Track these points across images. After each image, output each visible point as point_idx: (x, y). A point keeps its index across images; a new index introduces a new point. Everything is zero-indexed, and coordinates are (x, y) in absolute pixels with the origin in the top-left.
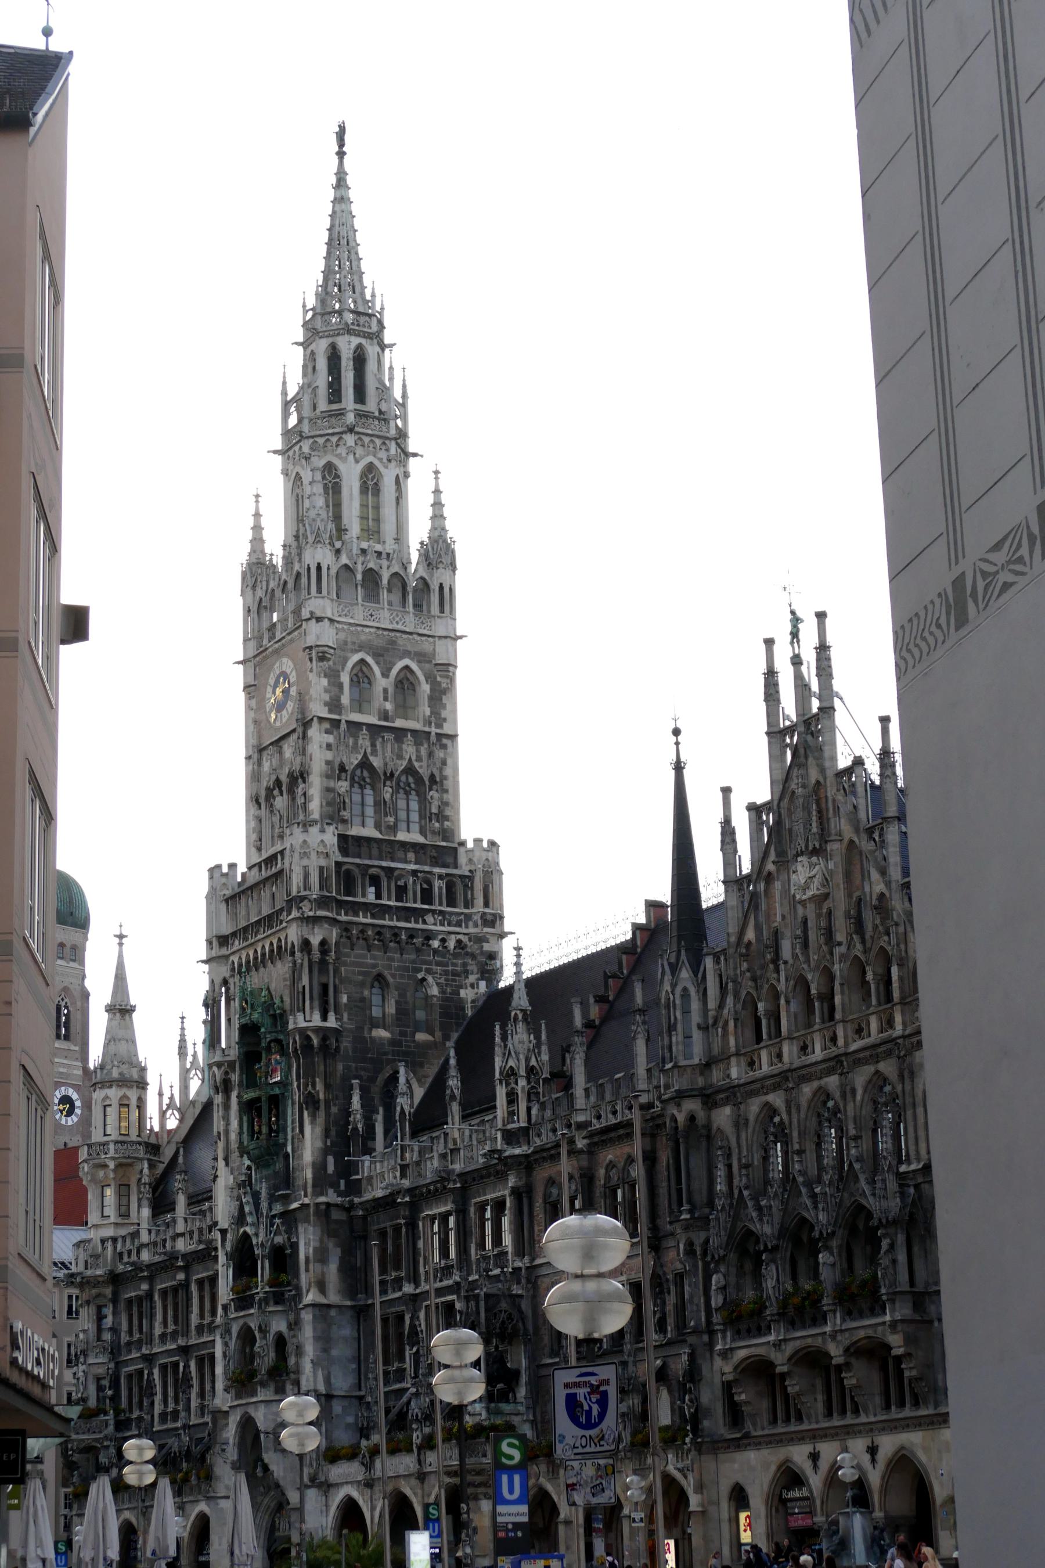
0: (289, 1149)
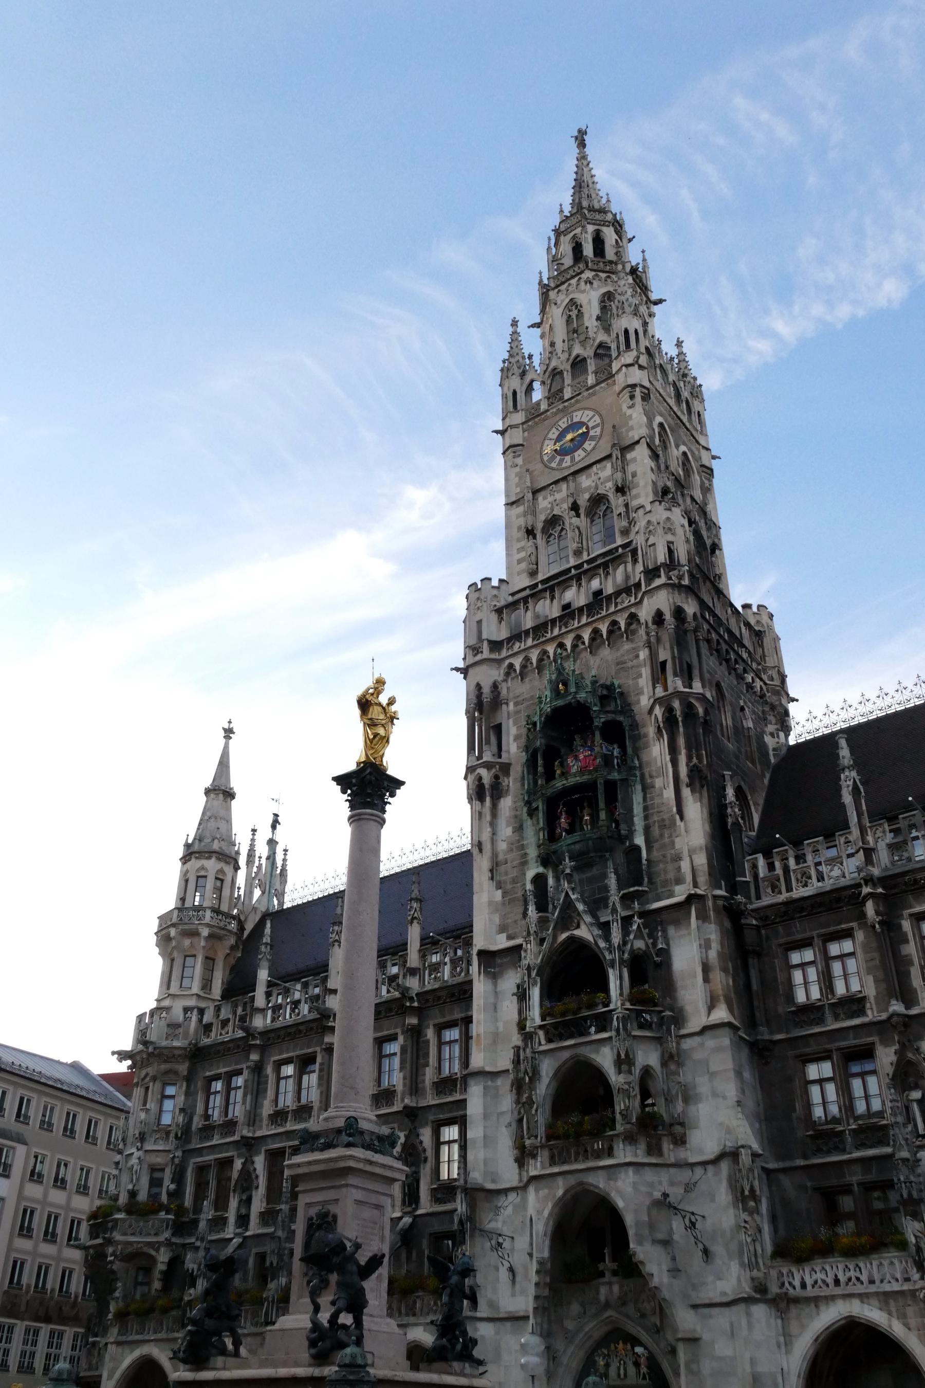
0: (639, 840)
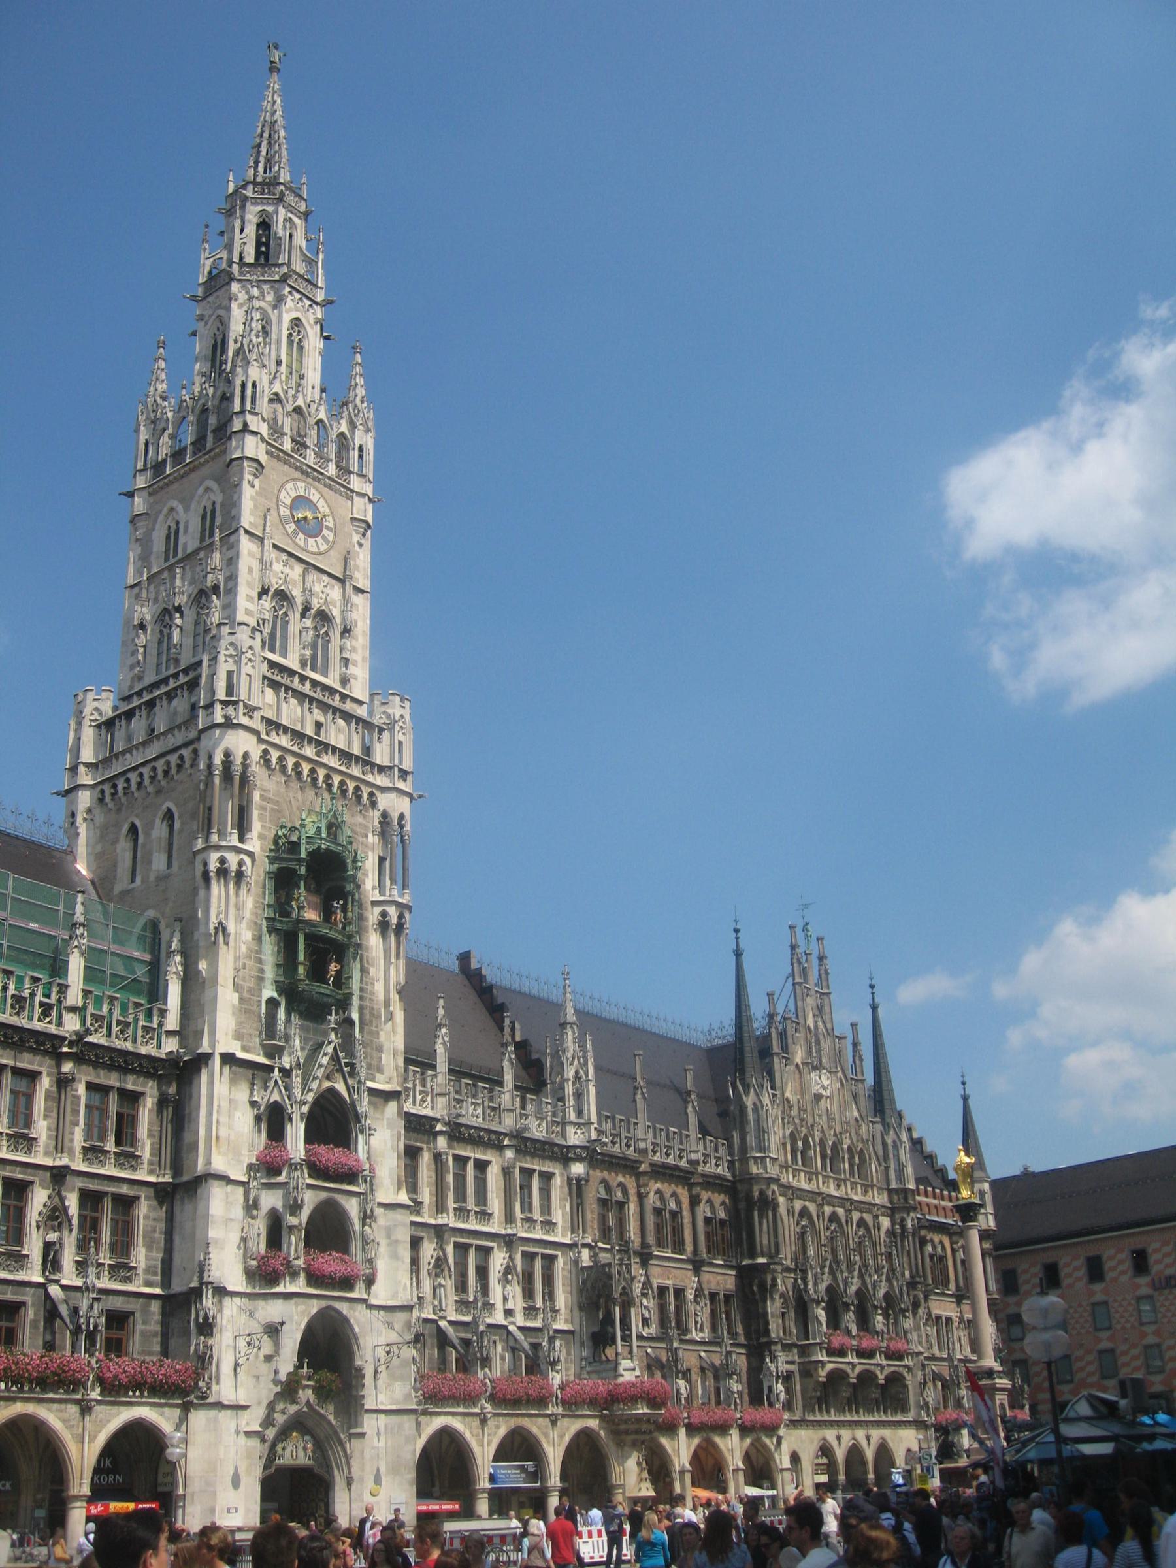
0: (355, 1016)
